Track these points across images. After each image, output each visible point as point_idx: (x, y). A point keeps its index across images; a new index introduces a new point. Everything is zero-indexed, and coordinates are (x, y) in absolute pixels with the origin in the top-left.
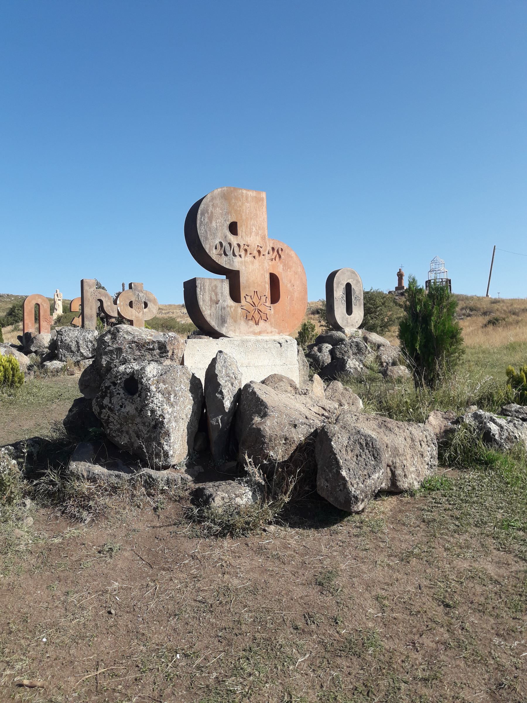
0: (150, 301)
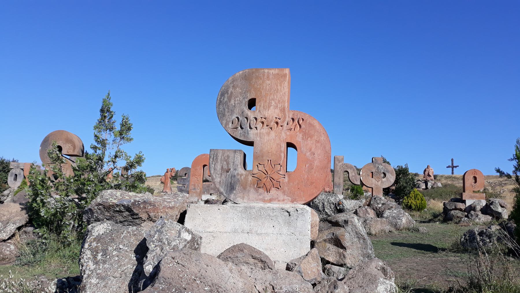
0: (388, 172)
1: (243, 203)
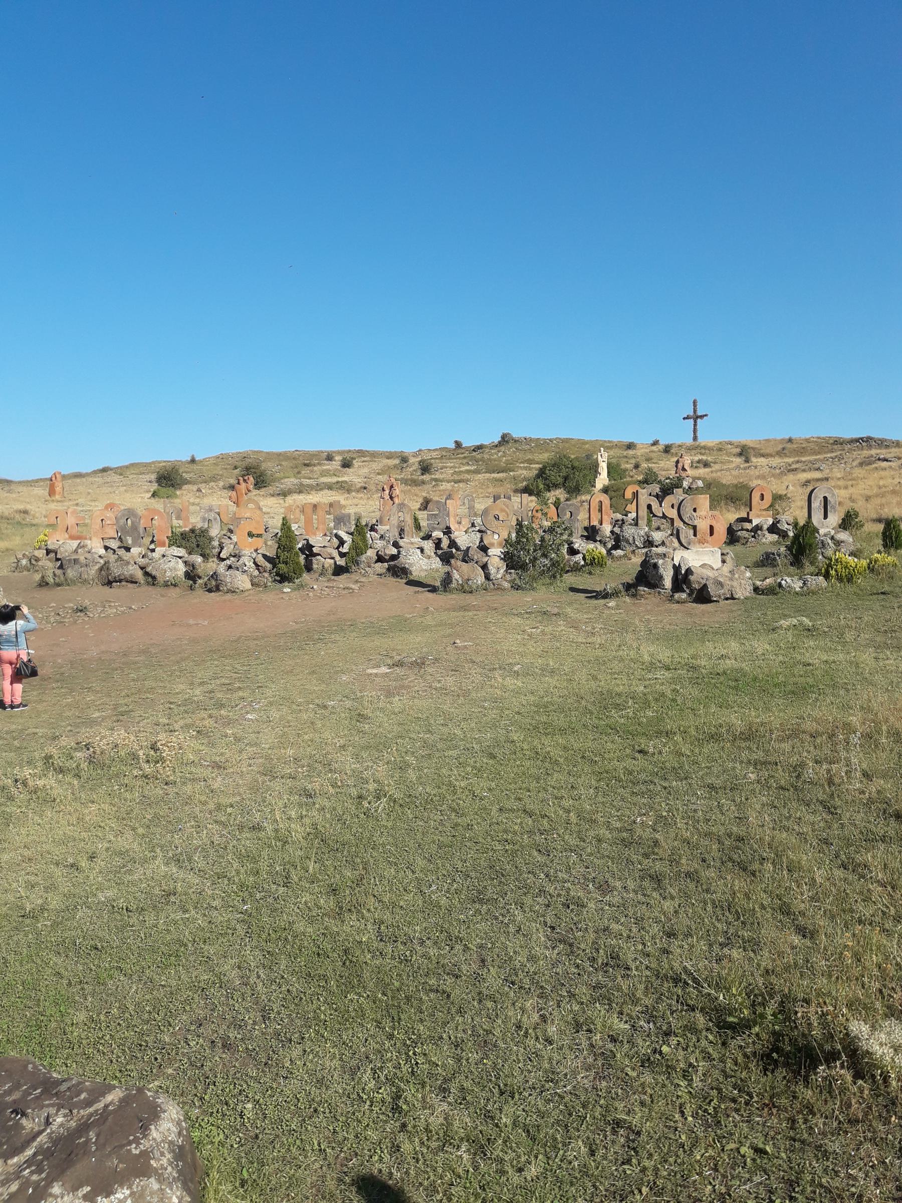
1: (694, 549)
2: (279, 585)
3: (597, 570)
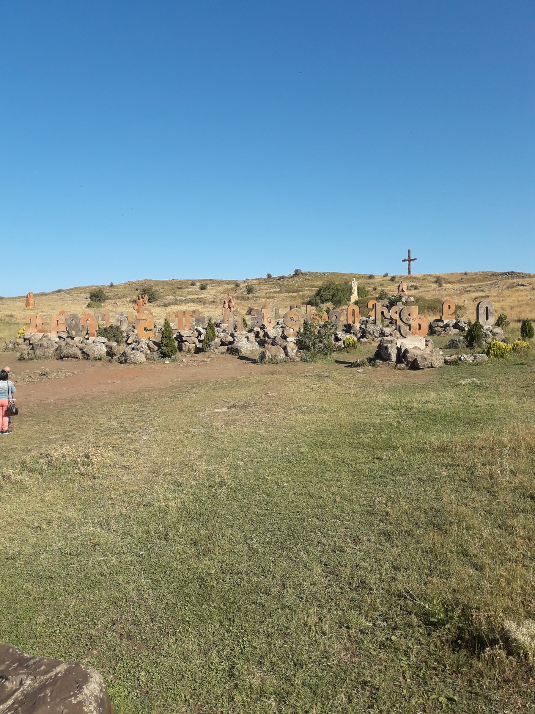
2: (162, 359)
3: (352, 350)
